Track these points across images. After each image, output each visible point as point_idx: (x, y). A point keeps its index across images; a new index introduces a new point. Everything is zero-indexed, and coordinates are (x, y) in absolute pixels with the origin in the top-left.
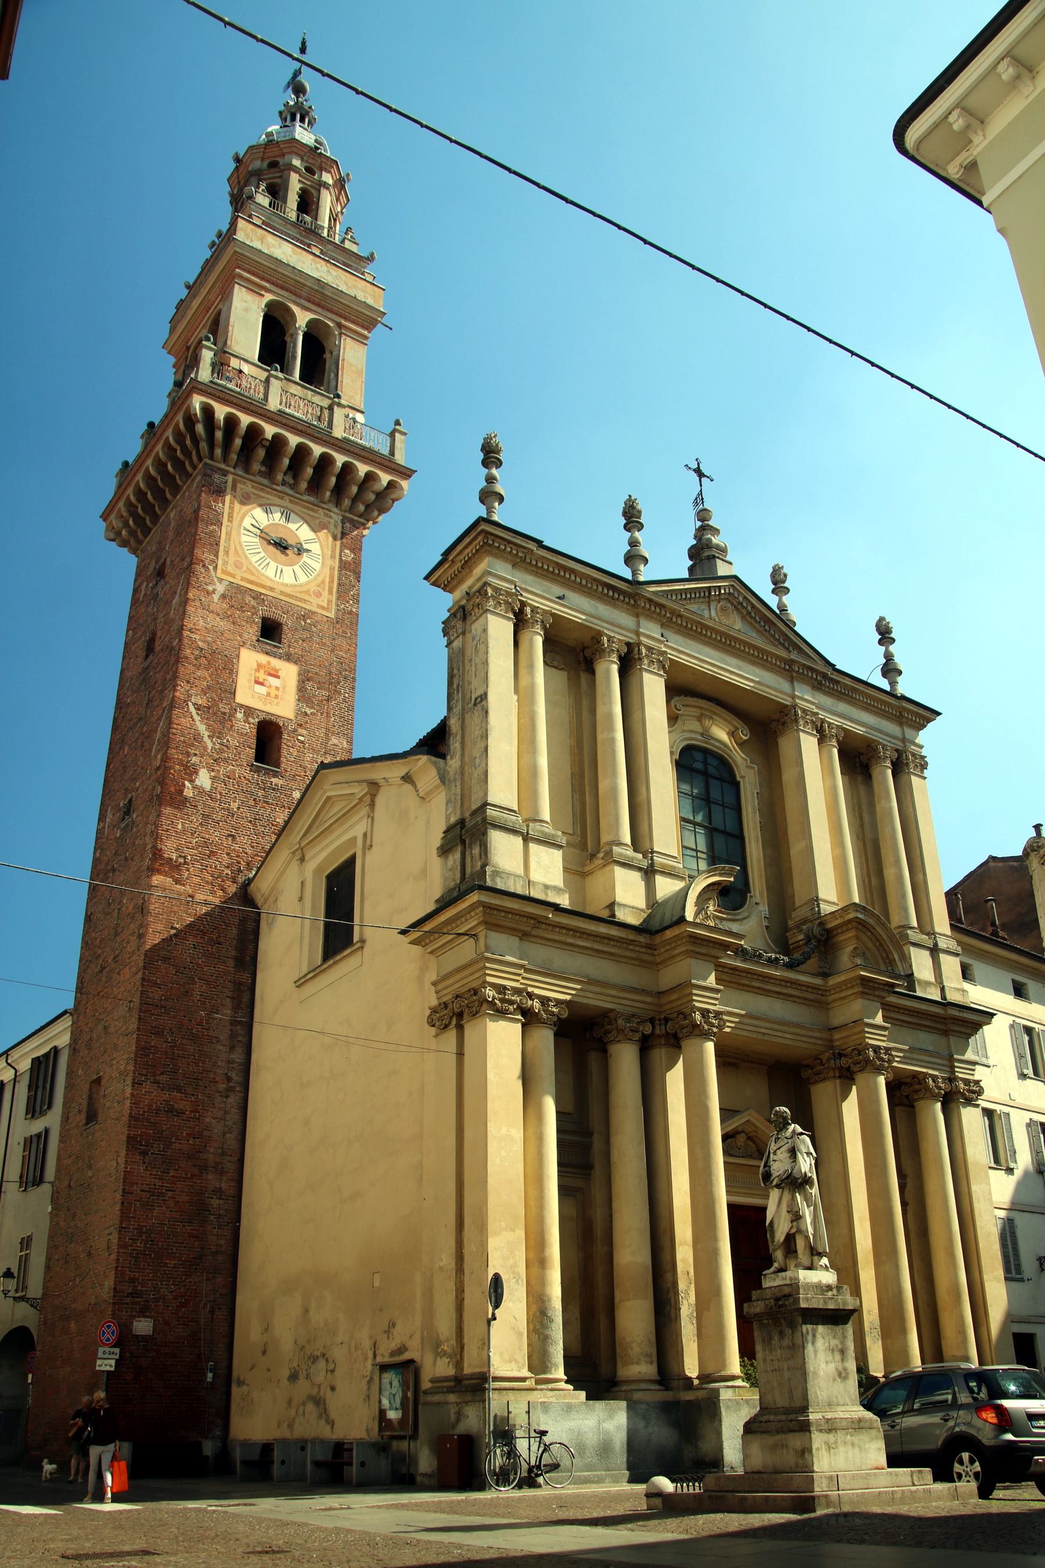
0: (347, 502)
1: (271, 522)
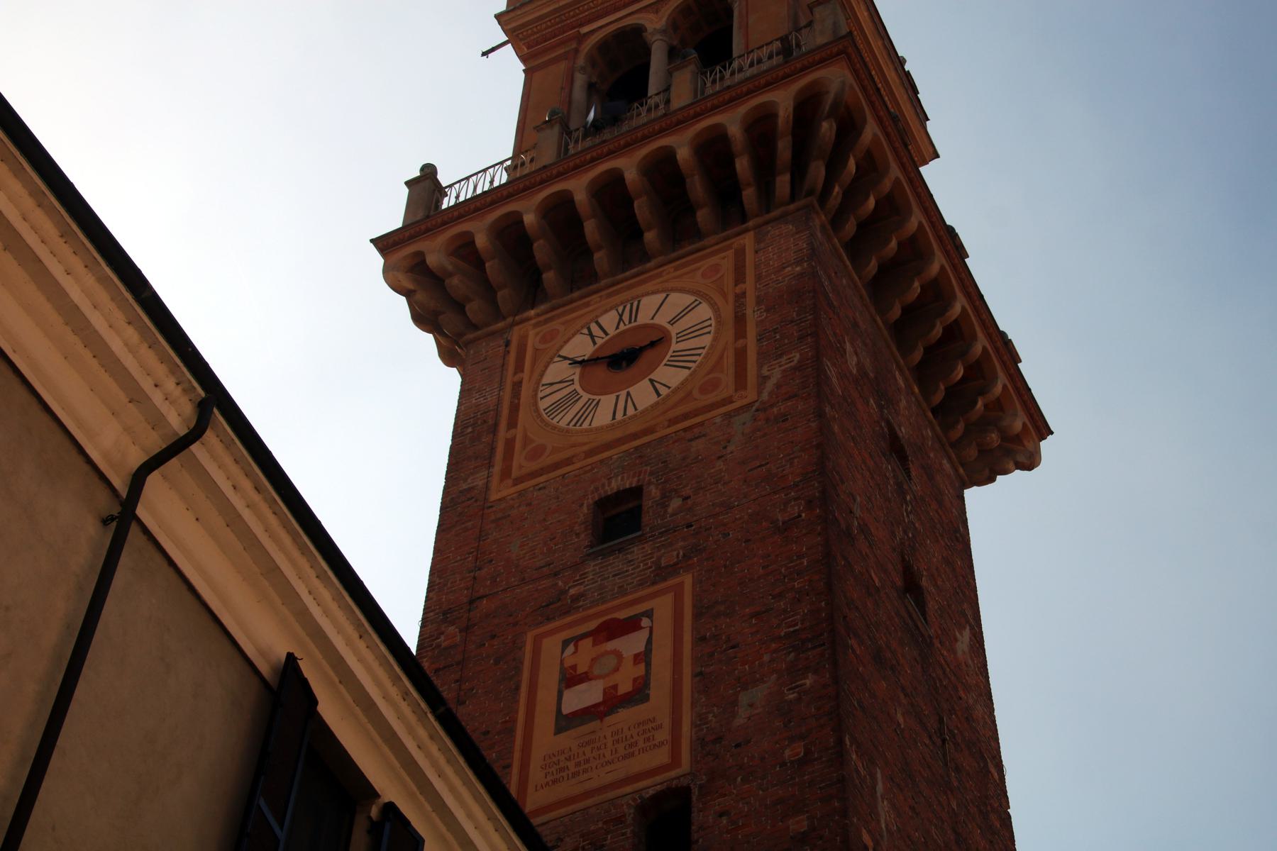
1: (599, 342)
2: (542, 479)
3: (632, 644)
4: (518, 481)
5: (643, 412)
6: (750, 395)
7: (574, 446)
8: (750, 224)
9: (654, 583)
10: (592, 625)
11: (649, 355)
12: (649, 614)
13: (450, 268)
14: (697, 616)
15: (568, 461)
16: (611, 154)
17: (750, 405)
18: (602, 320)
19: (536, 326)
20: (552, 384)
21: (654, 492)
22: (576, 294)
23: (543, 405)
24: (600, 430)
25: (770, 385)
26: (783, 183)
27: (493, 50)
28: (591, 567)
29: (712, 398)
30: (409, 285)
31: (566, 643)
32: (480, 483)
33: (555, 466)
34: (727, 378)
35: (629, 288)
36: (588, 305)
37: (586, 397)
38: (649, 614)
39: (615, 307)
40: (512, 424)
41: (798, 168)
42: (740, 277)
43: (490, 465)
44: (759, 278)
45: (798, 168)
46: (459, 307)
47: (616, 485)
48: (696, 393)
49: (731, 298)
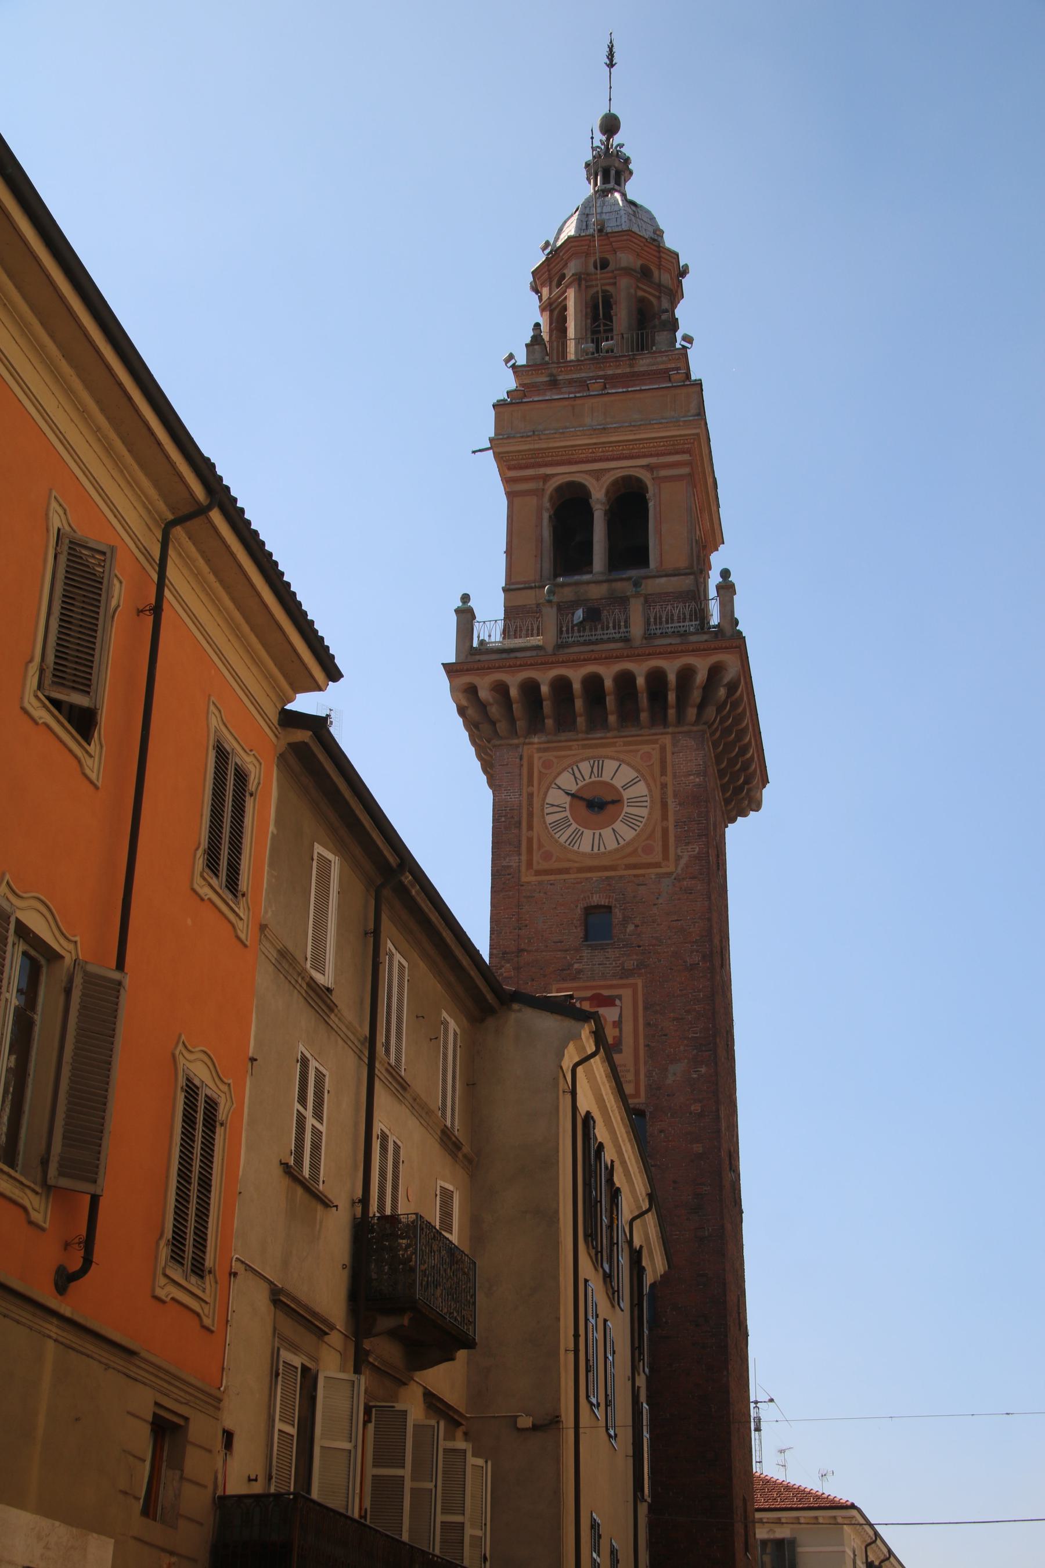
0: (672, 712)
1: (581, 784)
2: (552, 877)
4: (538, 873)
5: (610, 852)
7: (569, 860)
8: (670, 730)
9: (621, 978)
10: (589, 993)
11: (611, 808)
12: (620, 997)
13: (491, 700)
14: (646, 1008)
15: (566, 871)
16: (596, 660)
17: (669, 875)
18: (581, 765)
19: (539, 750)
20: (553, 805)
21: (618, 914)
22: (563, 736)
23: (549, 819)
24: (584, 854)
25: (683, 862)
26: (692, 713)
27: (480, 451)
28: (586, 953)
30: (465, 703)
32: (514, 865)
33: (560, 871)
34: (658, 848)
35: (596, 746)
36: (570, 748)
37: (574, 826)
38: (620, 997)
39: (588, 759)
40: (530, 827)
41: (701, 707)
42: (663, 773)
43: (520, 854)
44: (675, 776)
45: (701, 707)
46: (493, 724)
47: (596, 900)
48: (640, 850)
49: (659, 787)
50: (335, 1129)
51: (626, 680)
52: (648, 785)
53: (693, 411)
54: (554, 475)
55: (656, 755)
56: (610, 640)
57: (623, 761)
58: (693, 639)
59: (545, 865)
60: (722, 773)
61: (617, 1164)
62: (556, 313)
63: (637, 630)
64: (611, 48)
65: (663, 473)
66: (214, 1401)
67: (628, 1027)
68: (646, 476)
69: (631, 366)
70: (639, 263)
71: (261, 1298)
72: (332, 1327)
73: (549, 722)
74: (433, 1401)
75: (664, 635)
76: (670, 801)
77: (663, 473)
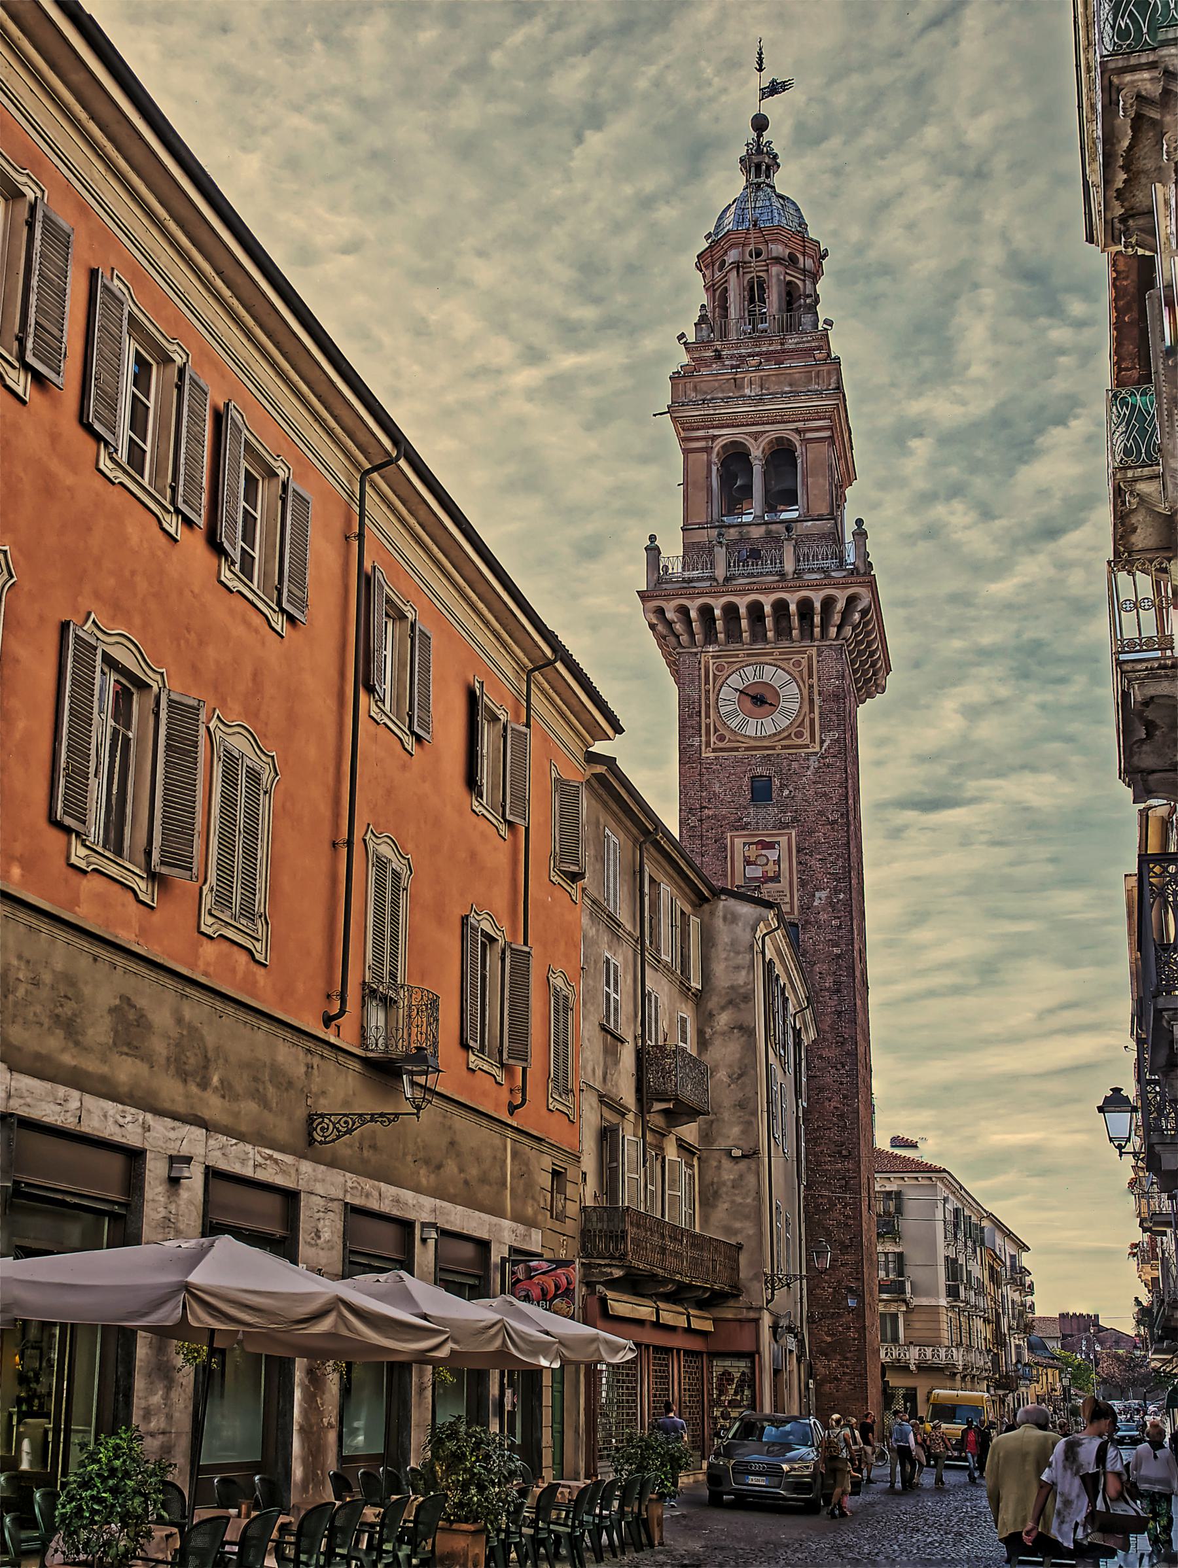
0: (817, 630)
3: (772, 855)
6: (817, 749)
10: (756, 839)
12: (778, 843)
14: (798, 852)
15: (736, 749)
16: (759, 591)
29: (799, 742)
31: (745, 844)
34: (807, 734)
36: (737, 656)
38: (778, 843)
42: (810, 676)
50: (624, 997)
51: (781, 607)
52: (799, 686)
53: (833, 386)
54: (720, 436)
55: (804, 662)
56: (768, 574)
57: (779, 667)
58: (833, 574)
59: (721, 745)
60: (855, 672)
61: (788, 985)
62: (718, 293)
63: (789, 567)
64: (760, 54)
65: (809, 435)
66: (578, 1159)
67: (784, 865)
68: (795, 438)
69: (782, 344)
70: (788, 251)
71: (594, 1101)
72: (630, 1111)
73: (721, 636)
74: (682, 1146)
75: (811, 571)
76: (816, 697)
77: (809, 435)
